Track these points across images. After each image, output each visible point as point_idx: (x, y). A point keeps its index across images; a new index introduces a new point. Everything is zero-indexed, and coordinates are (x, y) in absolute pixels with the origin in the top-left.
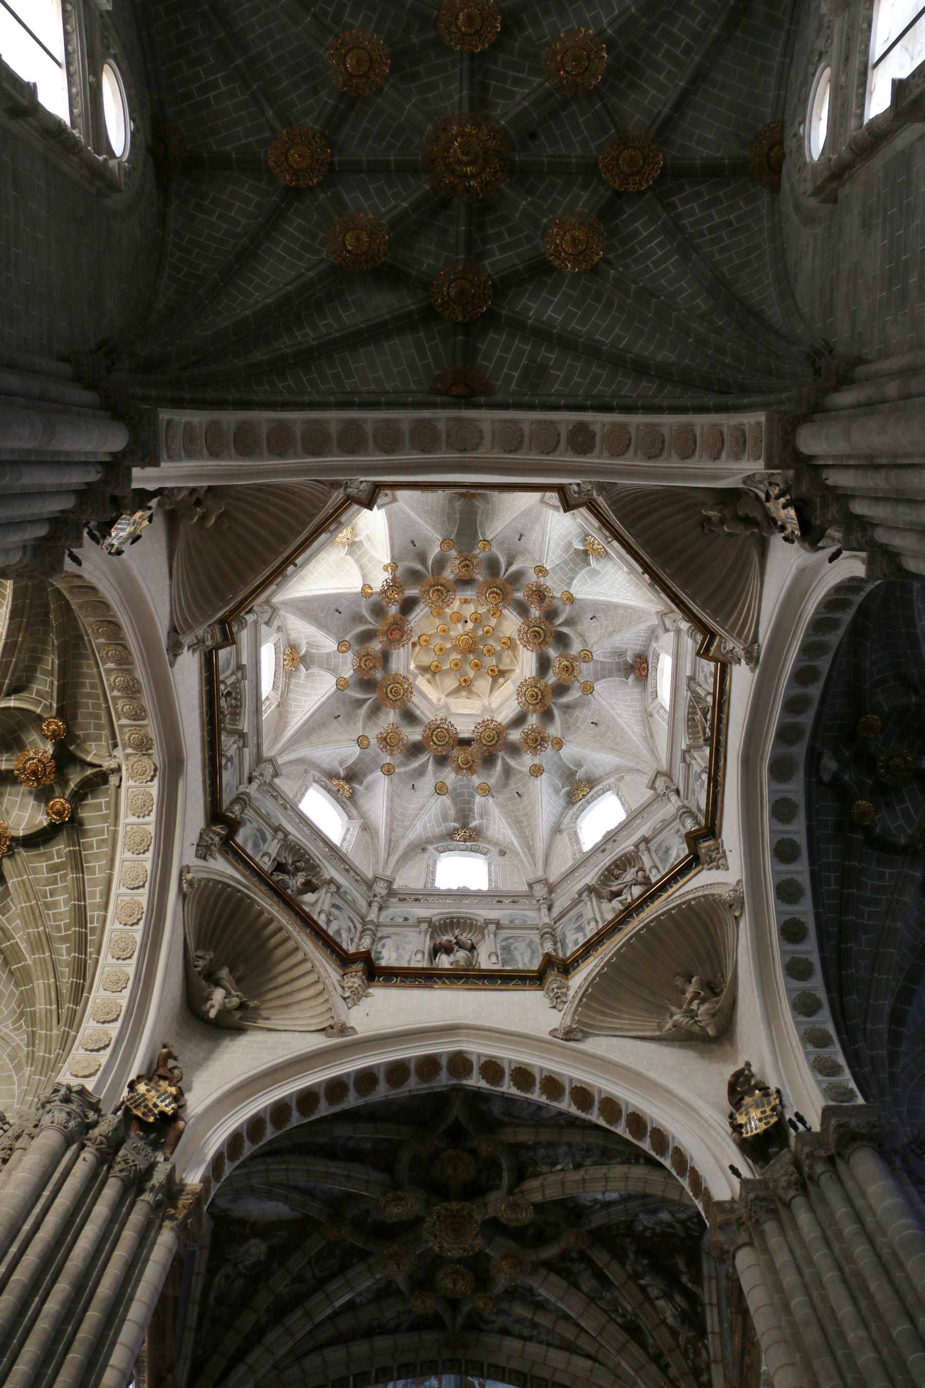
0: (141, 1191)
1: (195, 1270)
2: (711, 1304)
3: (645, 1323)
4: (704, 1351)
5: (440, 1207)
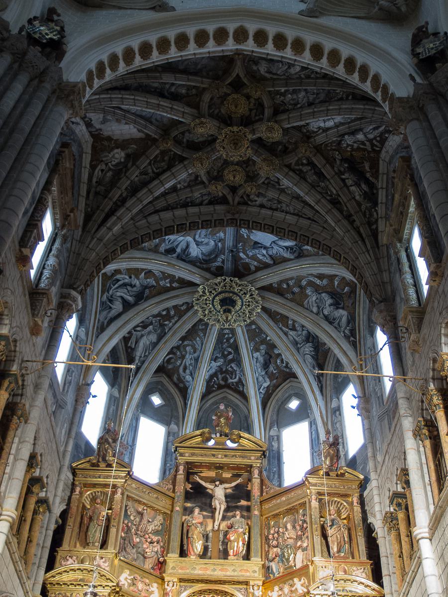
0: (41, 82)
1: (83, 165)
2: (382, 188)
3: (343, 199)
4: (375, 213)
5: (227, 130)
